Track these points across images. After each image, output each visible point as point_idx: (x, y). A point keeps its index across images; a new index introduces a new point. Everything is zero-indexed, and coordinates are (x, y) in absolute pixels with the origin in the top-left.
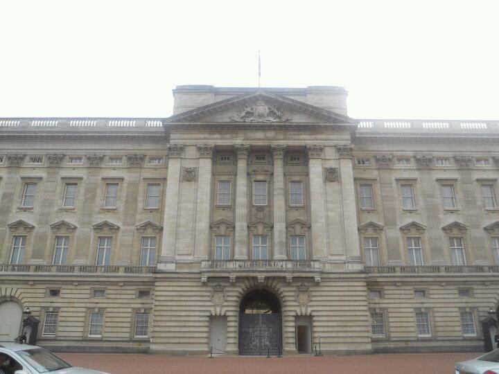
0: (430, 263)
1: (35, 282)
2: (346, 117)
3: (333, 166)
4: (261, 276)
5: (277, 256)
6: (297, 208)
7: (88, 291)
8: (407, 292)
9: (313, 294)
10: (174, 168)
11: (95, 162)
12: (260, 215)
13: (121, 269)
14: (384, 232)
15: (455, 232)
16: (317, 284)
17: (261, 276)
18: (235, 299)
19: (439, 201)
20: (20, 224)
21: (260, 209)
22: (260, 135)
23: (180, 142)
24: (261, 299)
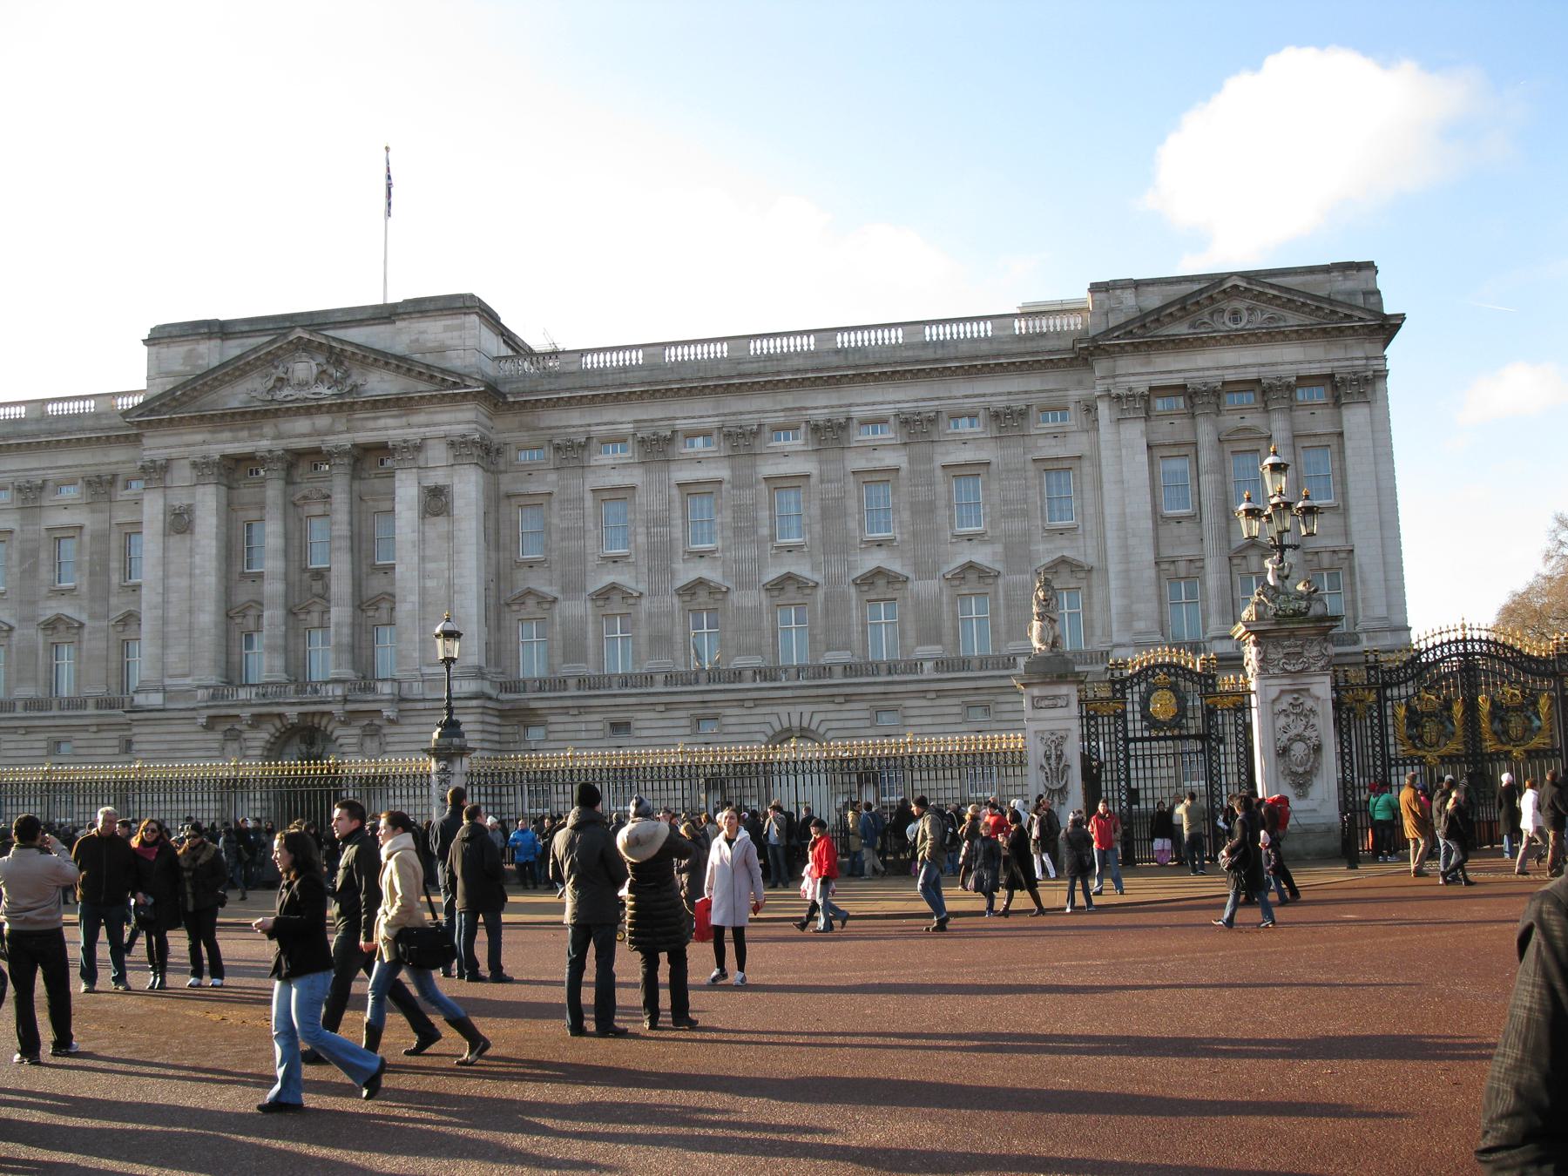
0: (646, 667)
2: (460, 375)
3: (441, 482)
5: (333, 673)
7: (44, 744)
8: (591, 726)
9: (389, 739)
12: (317, 587)
13: (91, 702)
14: (557, 606)
16: (391, 722)
17: (292, 713)
18: (258, 752)
19: (678, 533)
21: (320, 575)
22: (302, 425)
23: (159, 455)
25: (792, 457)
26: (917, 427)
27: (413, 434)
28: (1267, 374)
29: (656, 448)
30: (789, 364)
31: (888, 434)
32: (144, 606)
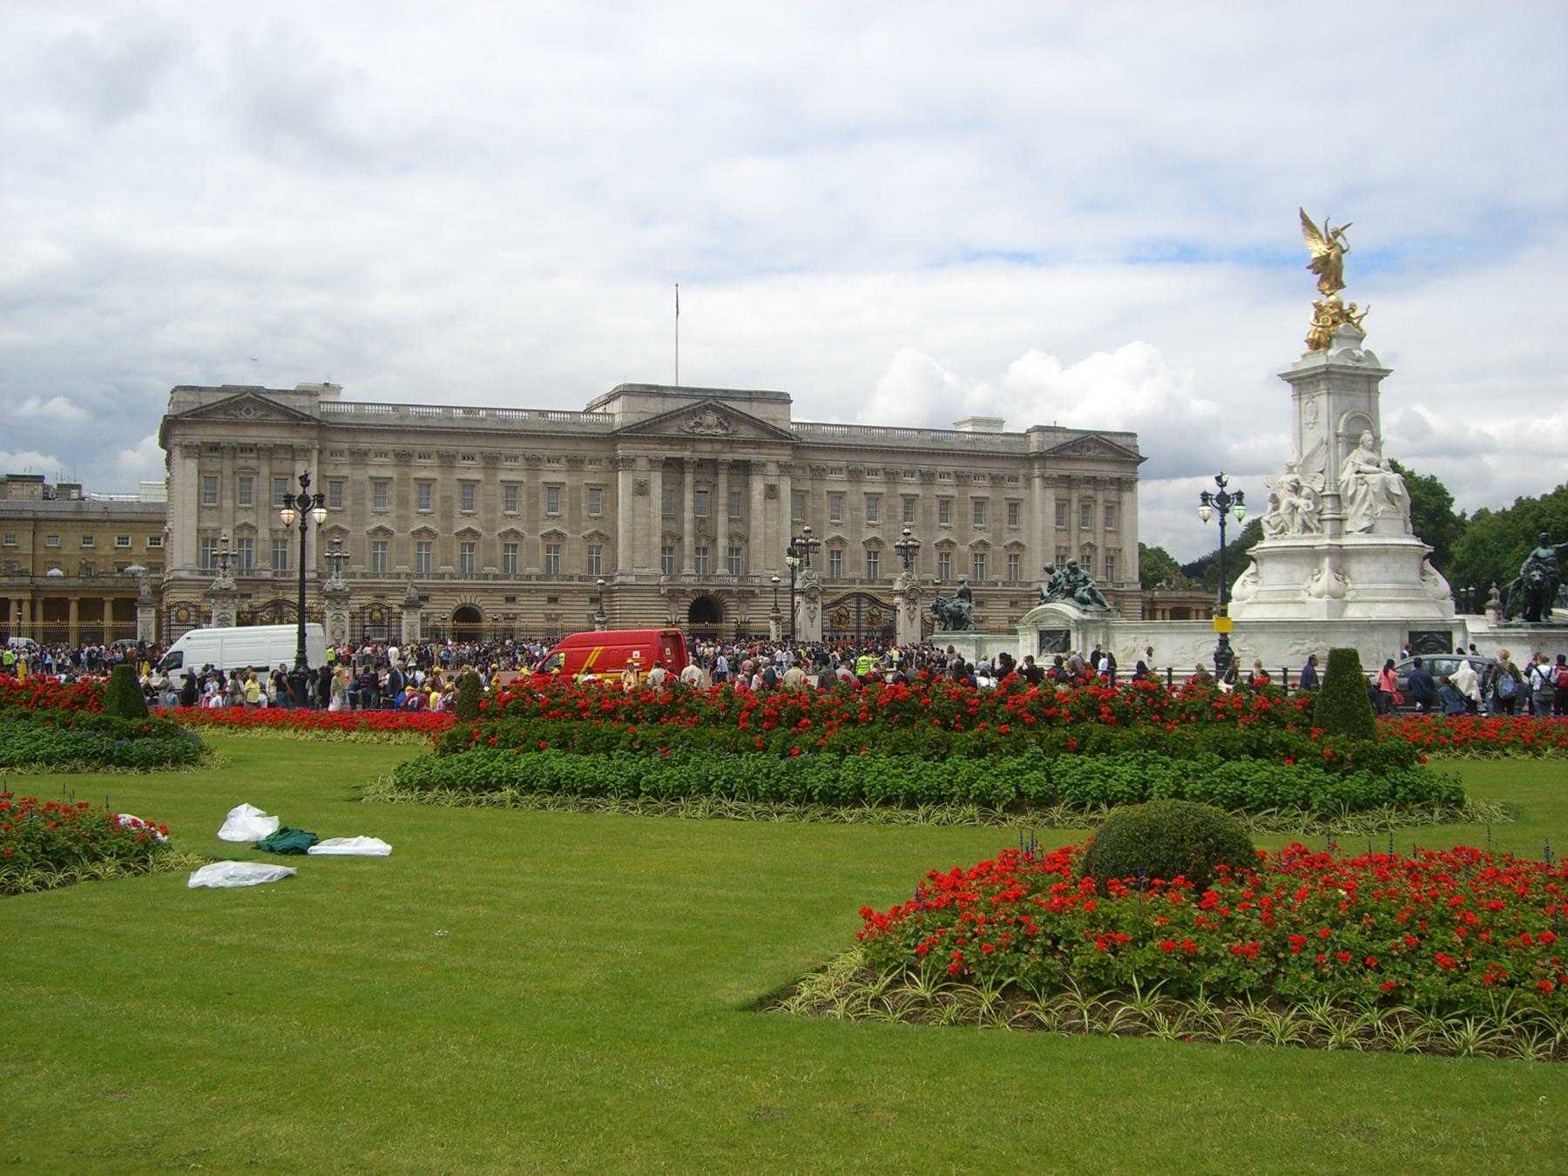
1: (495, 590)
2: (789, 436)
4: (712, 589)
5: (720, 571)
6: (735, 521)
10: (624, 480)
11: (533, 463)
12: (702, 527)
15: (874, 544)
16: (756, 596)
17: (712, 589)
19: (864, 515)
20: (469, 530)
21: (702, 521)
22: (707, 447)
23: (631, 453)
24: (706, 609)
25: (911, 487)
26: (962, 479)
27: (762, 458)
28: (1099, 475)
29: (855, 475)
30: (912, 445)
31: (951, 481)
32: (620, 531)
